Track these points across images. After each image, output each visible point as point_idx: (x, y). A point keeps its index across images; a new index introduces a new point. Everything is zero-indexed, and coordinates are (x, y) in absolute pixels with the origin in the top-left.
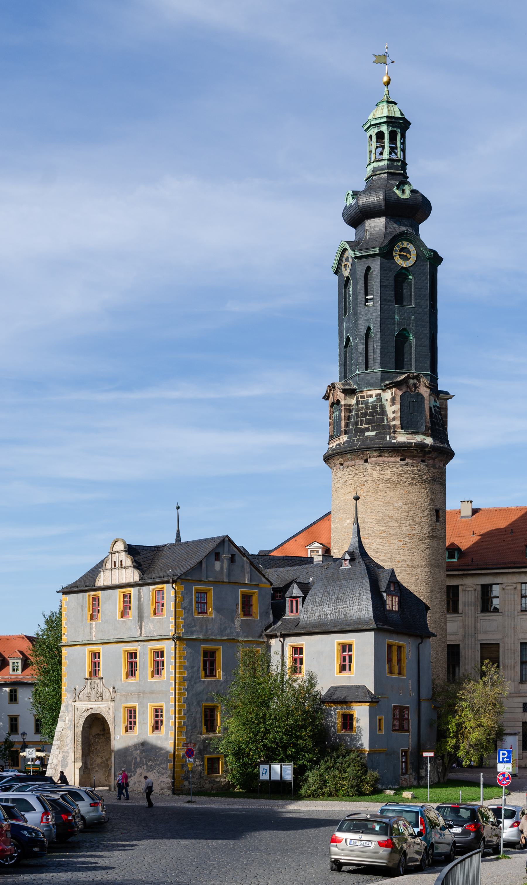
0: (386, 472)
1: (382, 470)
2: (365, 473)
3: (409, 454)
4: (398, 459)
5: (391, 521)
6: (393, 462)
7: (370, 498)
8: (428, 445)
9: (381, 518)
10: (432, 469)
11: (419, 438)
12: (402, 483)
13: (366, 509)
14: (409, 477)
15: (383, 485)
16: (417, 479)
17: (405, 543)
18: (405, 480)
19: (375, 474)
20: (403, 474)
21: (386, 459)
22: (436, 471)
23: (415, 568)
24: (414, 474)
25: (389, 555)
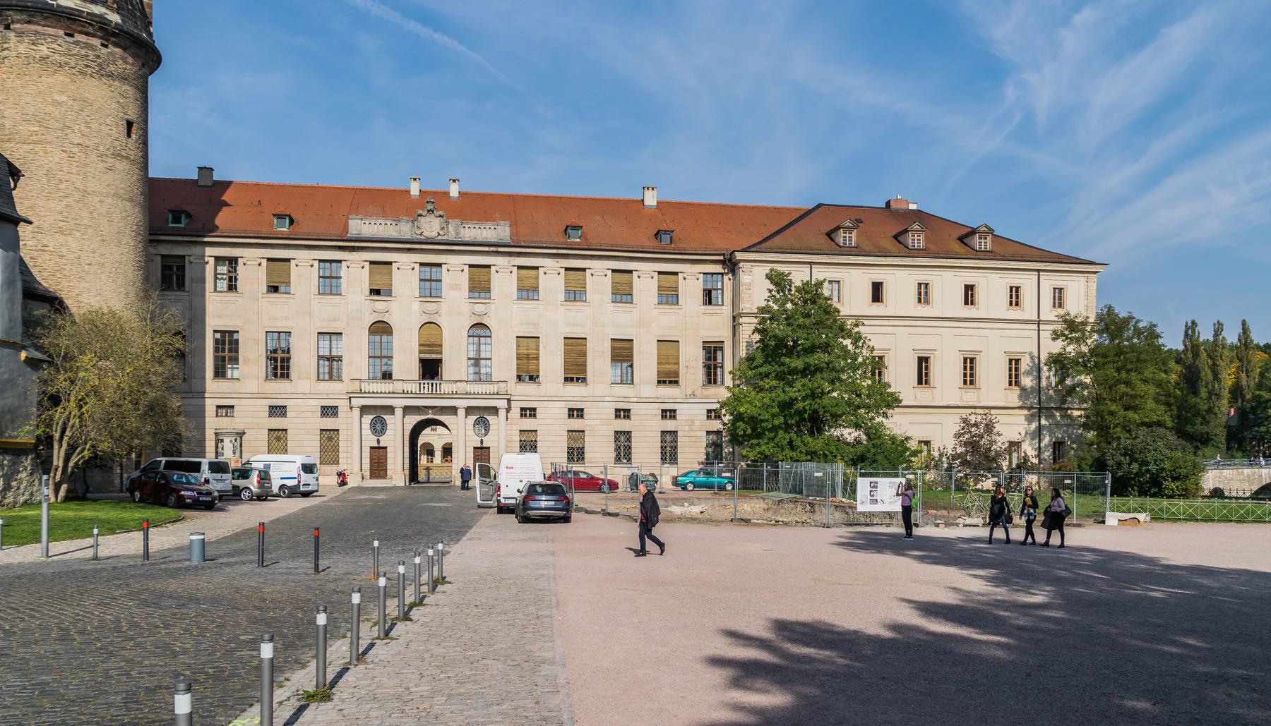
0: (41, 47)
1: (33, 44)
2: (6, 45)
3: (80, 28)
4: (61, 32)
5: (49, 120)
6: (53, 36)
7: (12, 82)
8: (111, 21)
9: (31, 113)
10: (121, 62)
11: (97, 9)
12: (67, 68)
13: (6, 98)
14: (80, 63)
15: (35, 65)
16: (94, 68)
17: (72, 155)
18: (73, 65)
19: (22, 49)
20: (70, 55)
21: (39, 28)
22: (128, 67)
23: (88, 194)
24: (88, 60)
25: (45, 169)
